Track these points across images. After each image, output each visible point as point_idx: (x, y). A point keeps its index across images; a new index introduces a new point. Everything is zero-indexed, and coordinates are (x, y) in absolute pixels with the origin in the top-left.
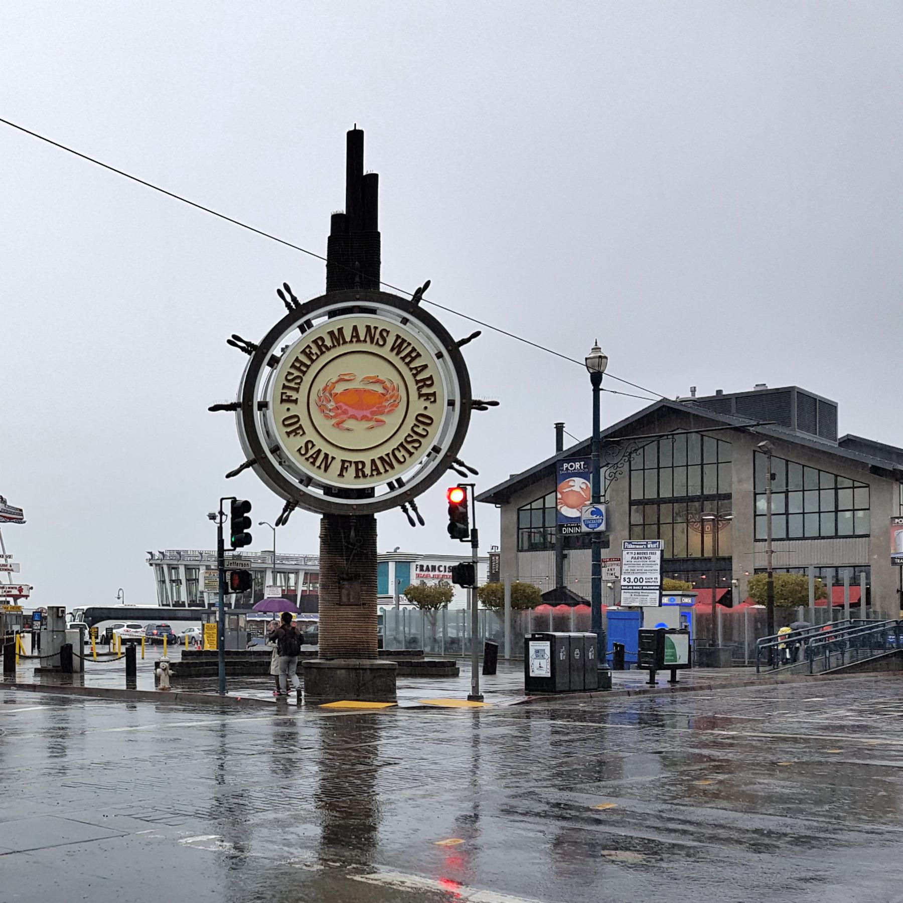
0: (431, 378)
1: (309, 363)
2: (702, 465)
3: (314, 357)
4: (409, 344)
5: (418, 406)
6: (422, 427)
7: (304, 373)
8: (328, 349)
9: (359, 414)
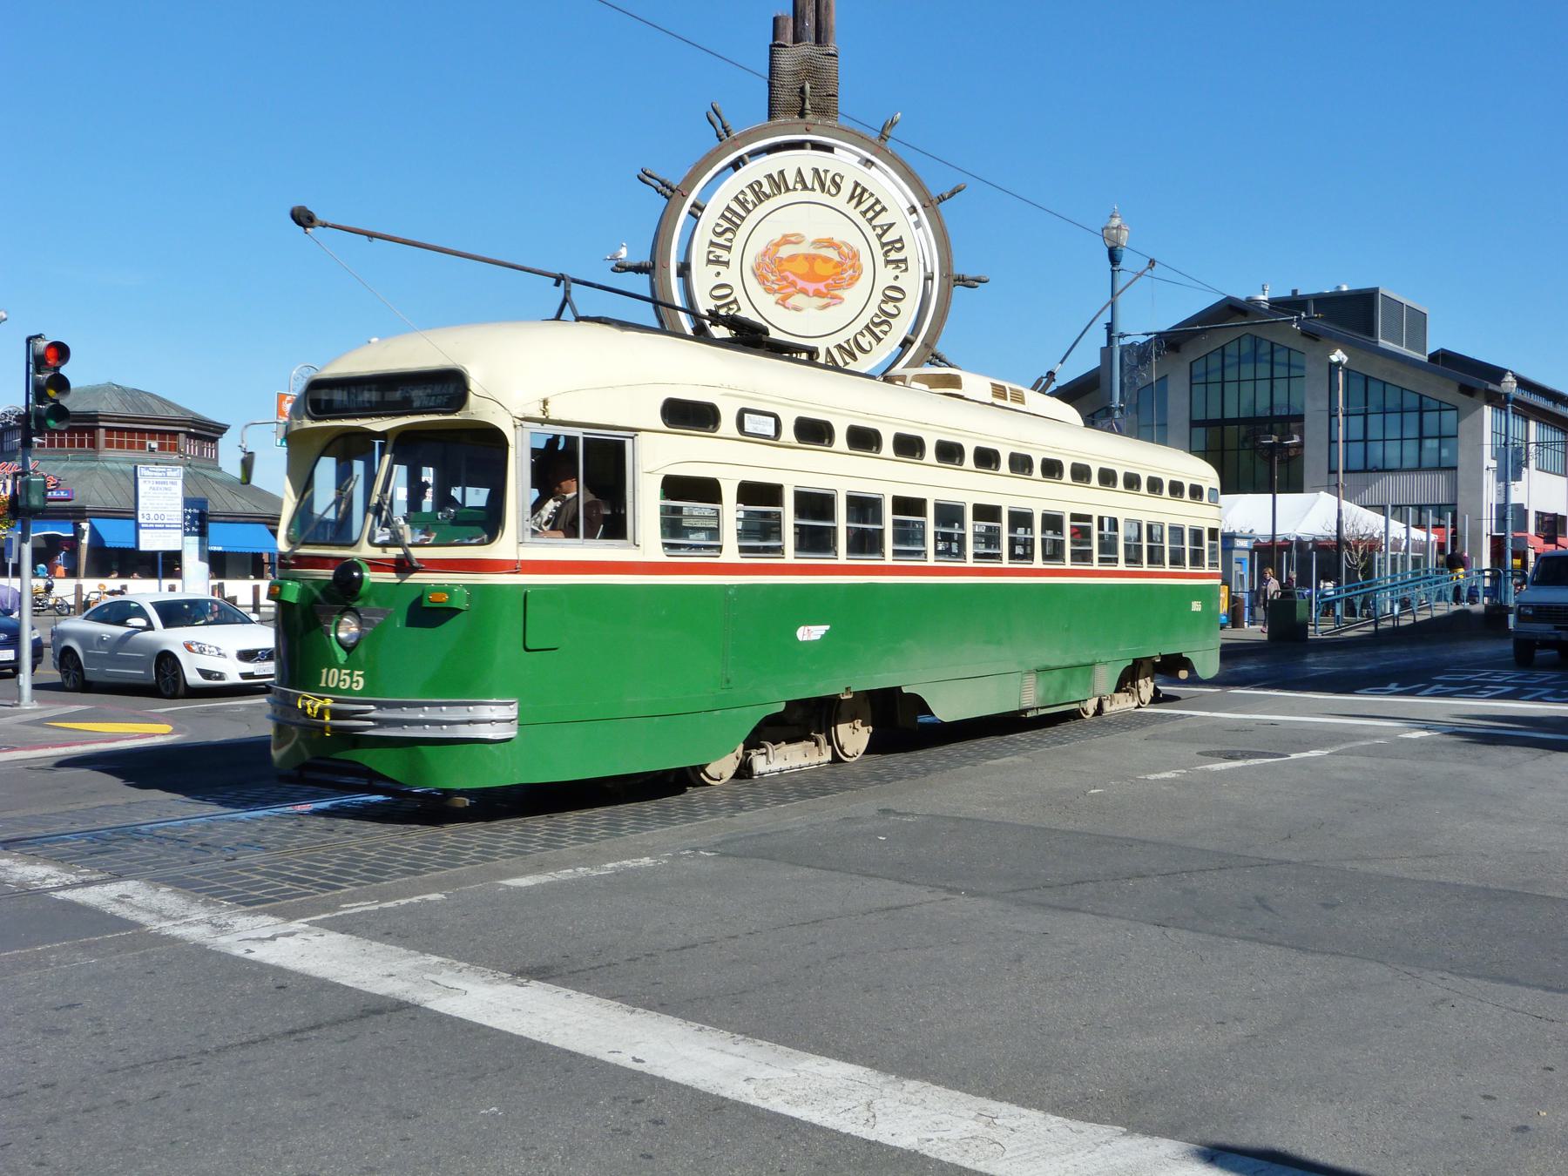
0: (900, 240)
1: (743, 213)
2: (1272, 379)
3: (750, 206)
4: (872, 195)
5: (886, 276)
6: (891, 304)
8: (768, 197)
9: (811, 287)
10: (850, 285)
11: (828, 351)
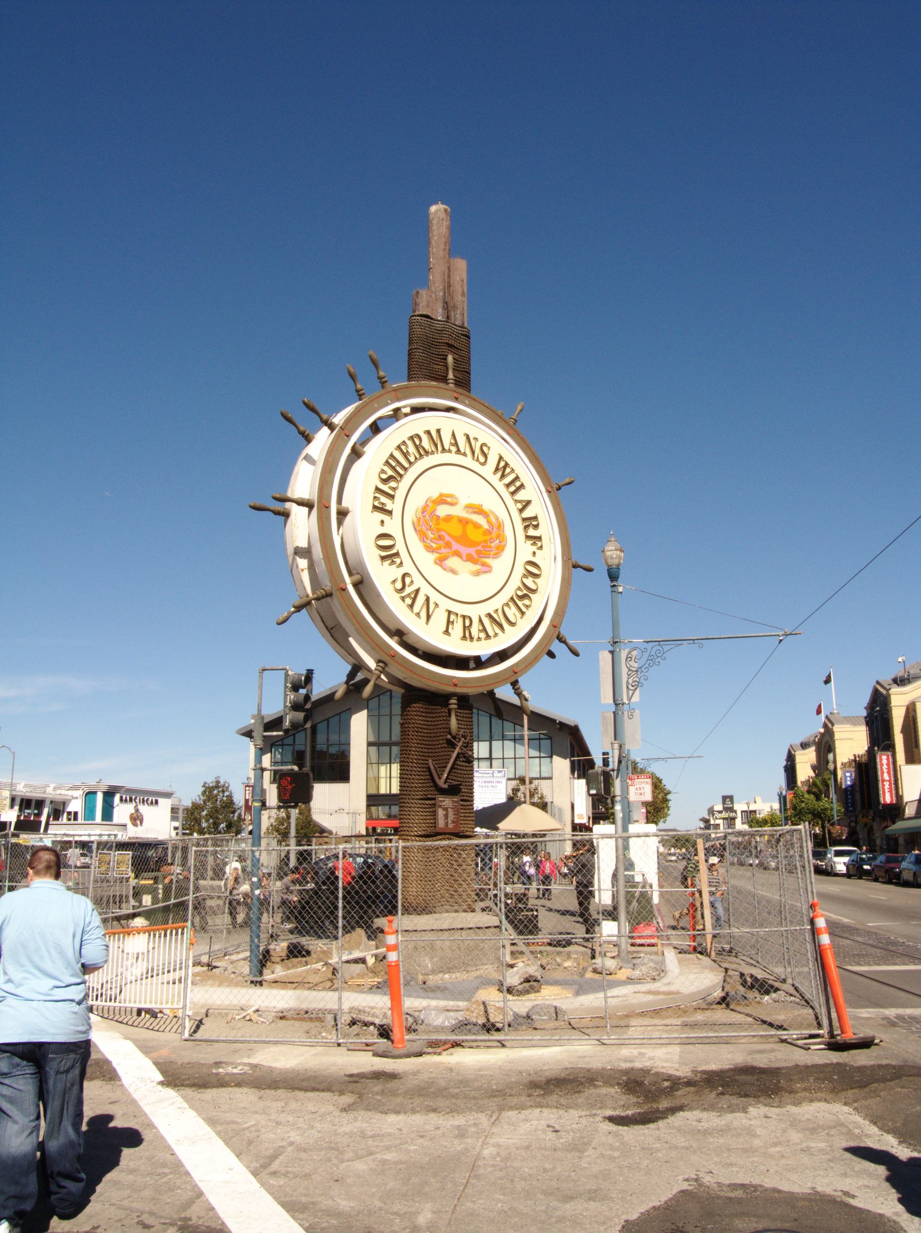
3: (412, 459)
4: (513, 471)
5: (526, 550)
6: (531, 579)
7: (401, 476)
8: (427, 453)
10: (497, 555)
11: (481, 621)
